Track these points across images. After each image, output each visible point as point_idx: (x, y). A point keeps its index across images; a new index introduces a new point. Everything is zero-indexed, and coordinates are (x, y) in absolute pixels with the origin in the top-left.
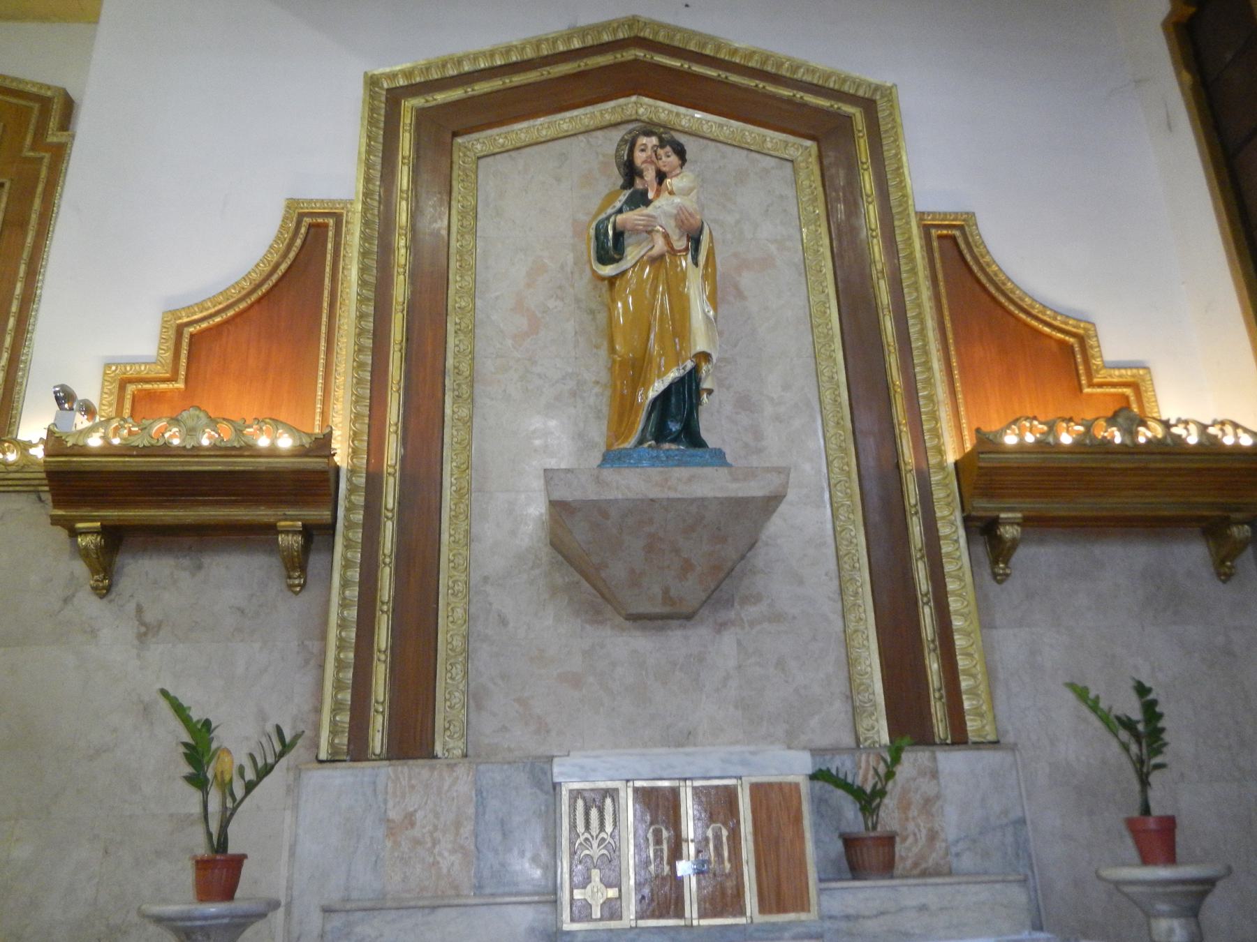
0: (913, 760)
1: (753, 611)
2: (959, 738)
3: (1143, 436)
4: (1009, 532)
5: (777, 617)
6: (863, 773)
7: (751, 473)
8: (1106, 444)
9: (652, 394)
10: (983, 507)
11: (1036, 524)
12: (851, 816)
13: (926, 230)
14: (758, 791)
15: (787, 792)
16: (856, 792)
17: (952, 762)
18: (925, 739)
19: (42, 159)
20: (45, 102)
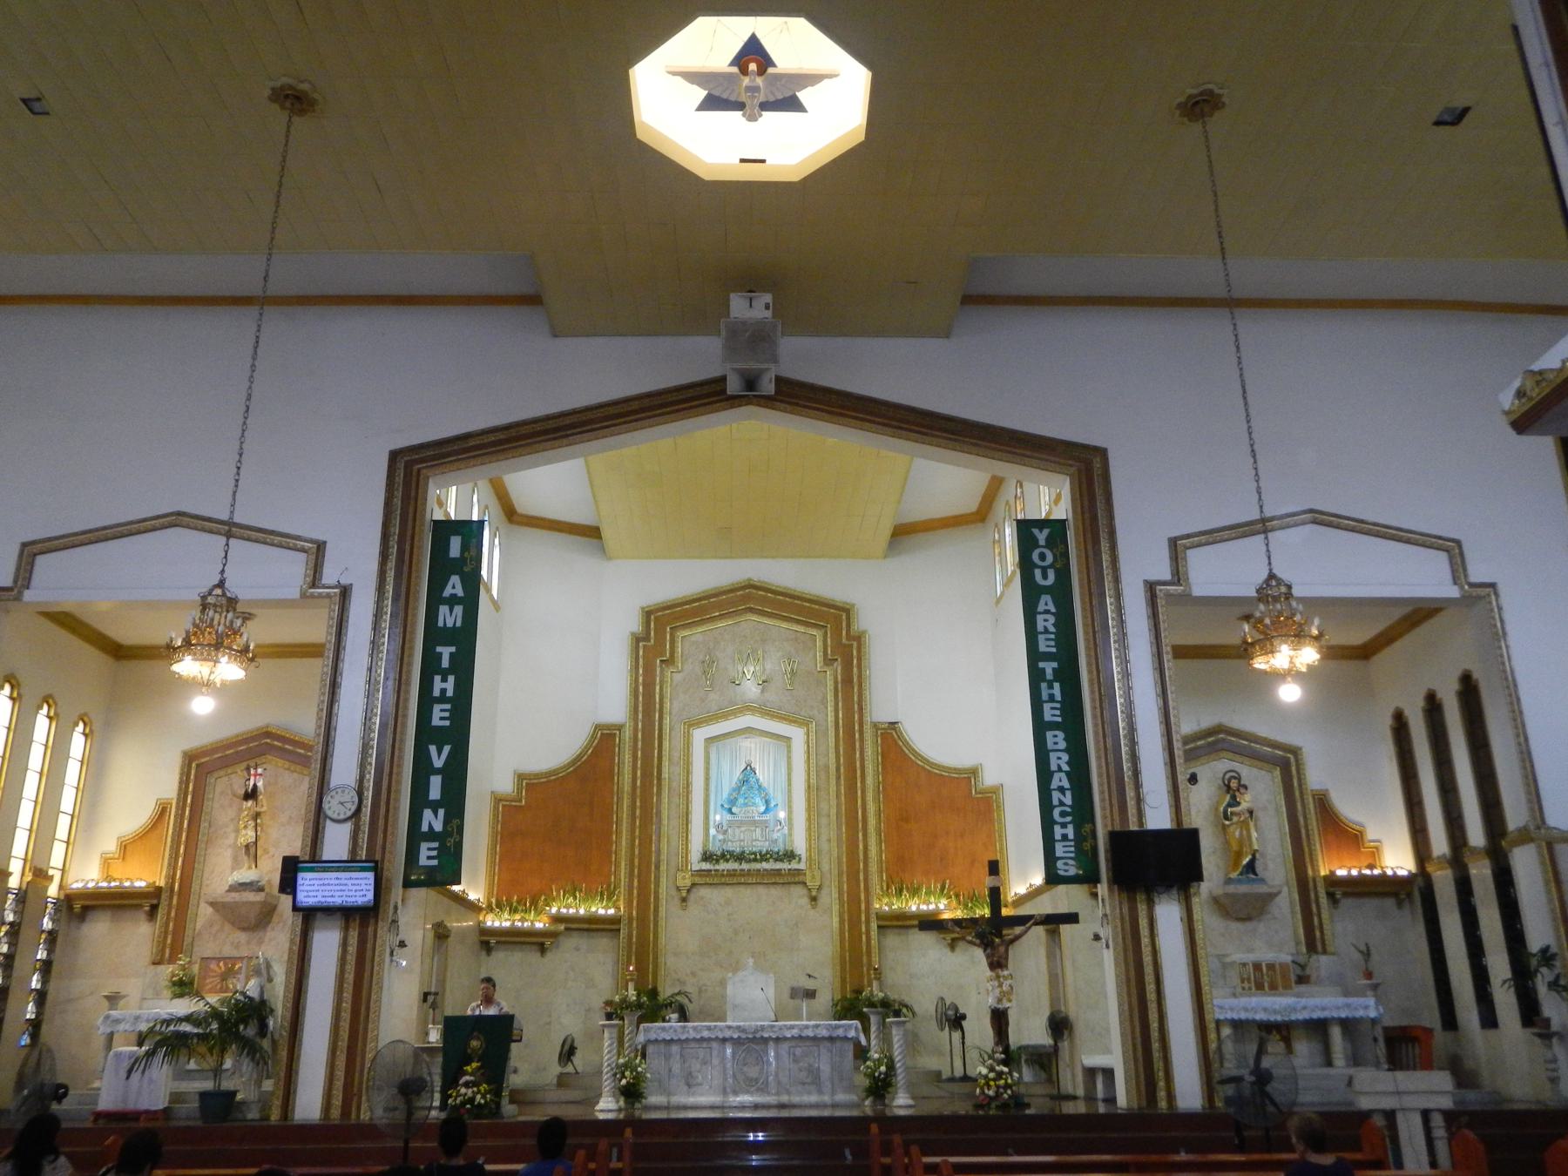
0: (1314, 957)
1: (1269, 916)
2: (1325, 952)
3: (1376, 872)
4: (1338, 896)
5: (1275, 918)
6: (1301, 960)
7: (1273, 887)
8: (1365, 876)
9: (1244, 862)
10: (1332, 890)
11: (1346, 895)
12: (1299, 971)
13: (1313, 796)
14: (1280, 964)
15: (1287, 965)
16: (1299, 965)
17: (1323, 959)
18: (1316, 952)
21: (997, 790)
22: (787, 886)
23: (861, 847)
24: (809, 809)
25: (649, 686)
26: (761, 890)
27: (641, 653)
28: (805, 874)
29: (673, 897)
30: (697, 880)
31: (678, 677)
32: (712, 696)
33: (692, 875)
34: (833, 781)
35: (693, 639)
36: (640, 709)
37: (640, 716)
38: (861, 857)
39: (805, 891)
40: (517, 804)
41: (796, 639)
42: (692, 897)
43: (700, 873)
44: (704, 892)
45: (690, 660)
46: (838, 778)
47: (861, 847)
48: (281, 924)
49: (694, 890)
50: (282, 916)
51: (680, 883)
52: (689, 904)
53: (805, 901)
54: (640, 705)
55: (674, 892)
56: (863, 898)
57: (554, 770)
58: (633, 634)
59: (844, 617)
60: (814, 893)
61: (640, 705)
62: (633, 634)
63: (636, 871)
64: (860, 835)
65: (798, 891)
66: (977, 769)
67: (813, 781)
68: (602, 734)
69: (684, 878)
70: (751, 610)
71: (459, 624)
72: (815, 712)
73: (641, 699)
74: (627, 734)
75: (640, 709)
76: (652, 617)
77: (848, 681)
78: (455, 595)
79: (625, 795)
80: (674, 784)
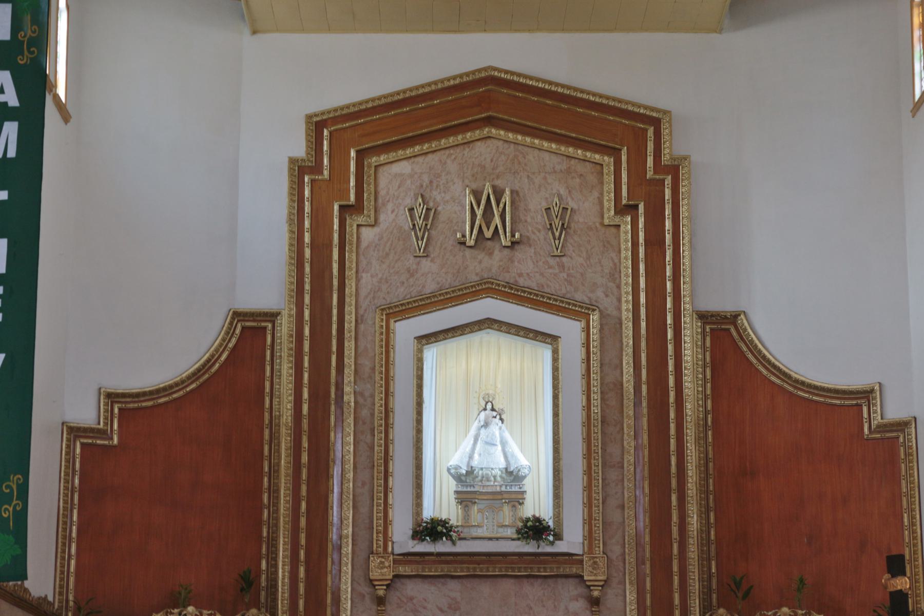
19: (664, 180)
20: (656, 123)
21: (902, 426)
22: (550, 581)
23: (675, 518)
24: (588, 455)
25: (321, 248)
26: (508, 585)
27: (307, 193)
28: (581, 562)
29: (363, 596)
30: (402, 570)
31: (368, 234)
32: (426, 264)
33: (395, 561)
34: (629, 411)
35: (396, 168)
36: (307, 287)
37: (307, 299)
38: (675, 530)
39: (581, 590)
40: (106, 442)
41: (568, 171)
42: (393, 597)
44: (412, 588)
45: (390, 206)
46: (637, 404)
47: (675, 518)
49: (398, 584)
51: (375, 574)
52: (388, 607)
53: (579, 606)
54: (307, 280)
55: (365, 589)
56: (677, 601)
57: (164, 389)
58: (292, 161)
59: (651, 132)
60: (596, 594)
61: (307, 280)
62: (292, 161)
63: (302, 553)
64: (674, 498)
65: (570, 589)
66: (872, 391)
67: (596, 409)
68: (243, 328)
69: (381, 566)
70: (490, 121)
71: (12, 153)
72: (600, 293)
73: (307, 269)
74: (285, 326)
75: (307, 287)
76: (326, 132)
77: (655, 242)
78: (6, 103)
79: (283, 431)
80: (365, 413)
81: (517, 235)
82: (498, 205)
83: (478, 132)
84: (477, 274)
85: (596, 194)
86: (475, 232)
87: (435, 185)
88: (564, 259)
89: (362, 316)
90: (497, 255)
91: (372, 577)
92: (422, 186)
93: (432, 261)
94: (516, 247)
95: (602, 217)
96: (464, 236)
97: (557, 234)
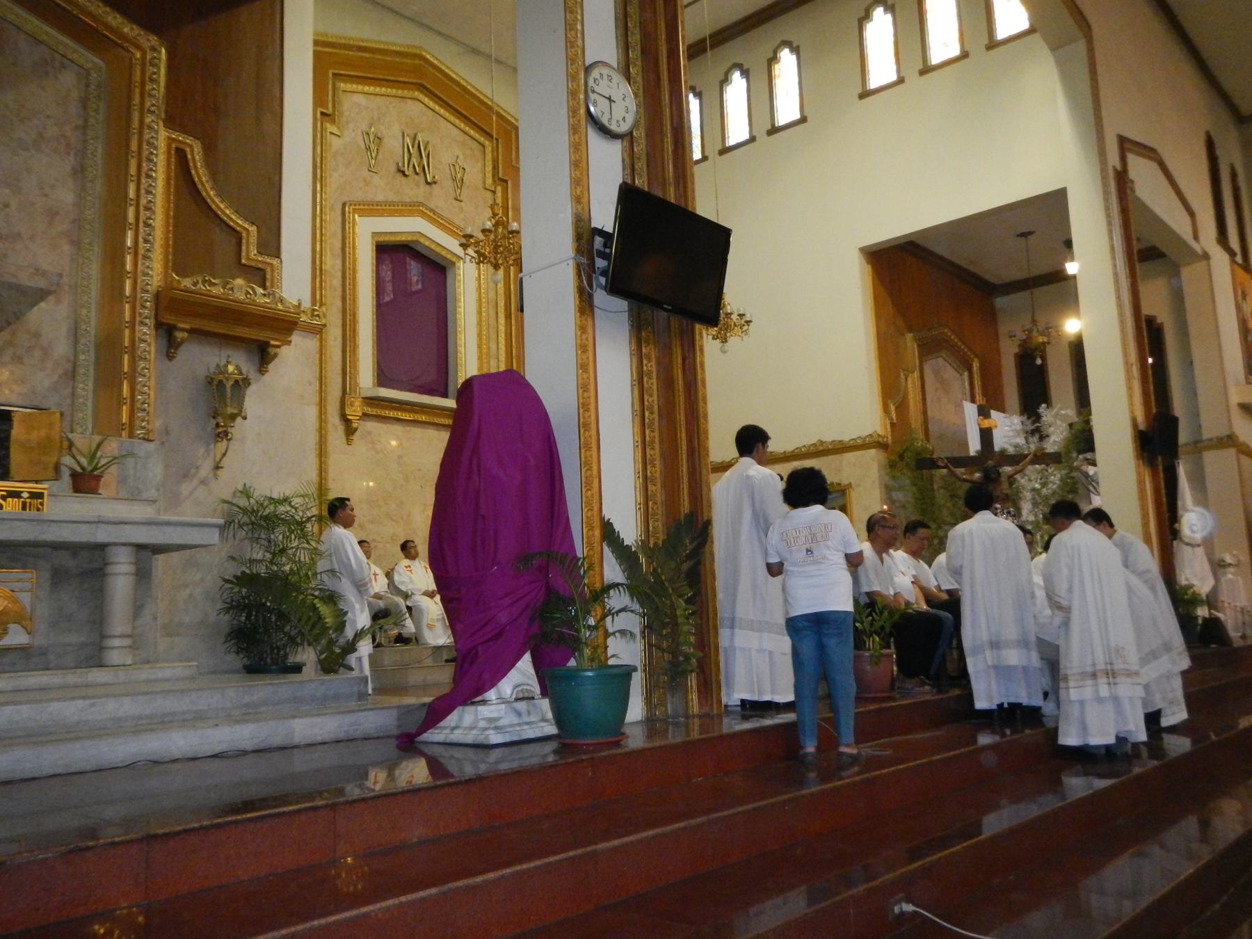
30: (370, 411)
32: (376, 180)
43: (371, 401)
44: (370, 425)
45: (351, 125)
48: (37, 354)
50: (37, 335)
81: (436, 177)
82: (425, 150)
83: (411, 92)
84: (410, 198)
85: (480, 165)
86: (411, 166)
87: (382, 121)
88: (462, 204)
89: (333, 205)
90: (424, 188)
91: (347, 413)
92: (373, 118)
93: (380, 178)
94: (434, 186)
95: (484, 183)
96: (404, 166)
97: (459, 186)
